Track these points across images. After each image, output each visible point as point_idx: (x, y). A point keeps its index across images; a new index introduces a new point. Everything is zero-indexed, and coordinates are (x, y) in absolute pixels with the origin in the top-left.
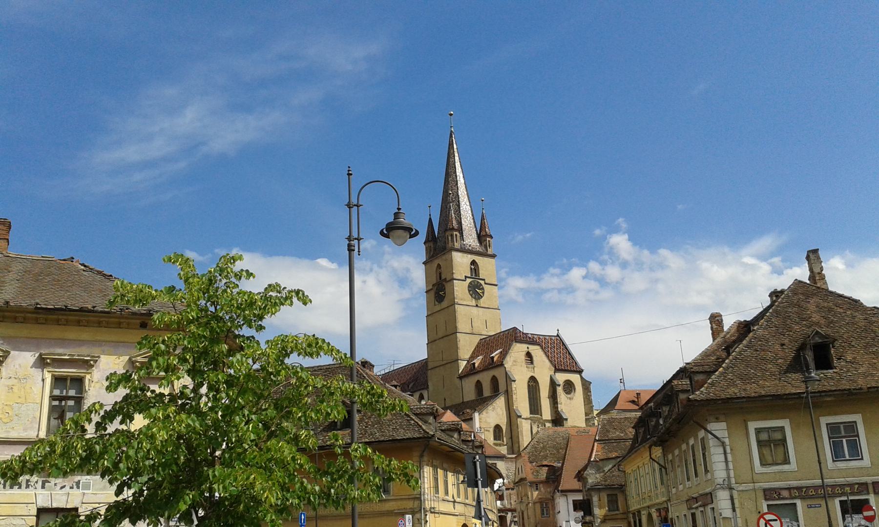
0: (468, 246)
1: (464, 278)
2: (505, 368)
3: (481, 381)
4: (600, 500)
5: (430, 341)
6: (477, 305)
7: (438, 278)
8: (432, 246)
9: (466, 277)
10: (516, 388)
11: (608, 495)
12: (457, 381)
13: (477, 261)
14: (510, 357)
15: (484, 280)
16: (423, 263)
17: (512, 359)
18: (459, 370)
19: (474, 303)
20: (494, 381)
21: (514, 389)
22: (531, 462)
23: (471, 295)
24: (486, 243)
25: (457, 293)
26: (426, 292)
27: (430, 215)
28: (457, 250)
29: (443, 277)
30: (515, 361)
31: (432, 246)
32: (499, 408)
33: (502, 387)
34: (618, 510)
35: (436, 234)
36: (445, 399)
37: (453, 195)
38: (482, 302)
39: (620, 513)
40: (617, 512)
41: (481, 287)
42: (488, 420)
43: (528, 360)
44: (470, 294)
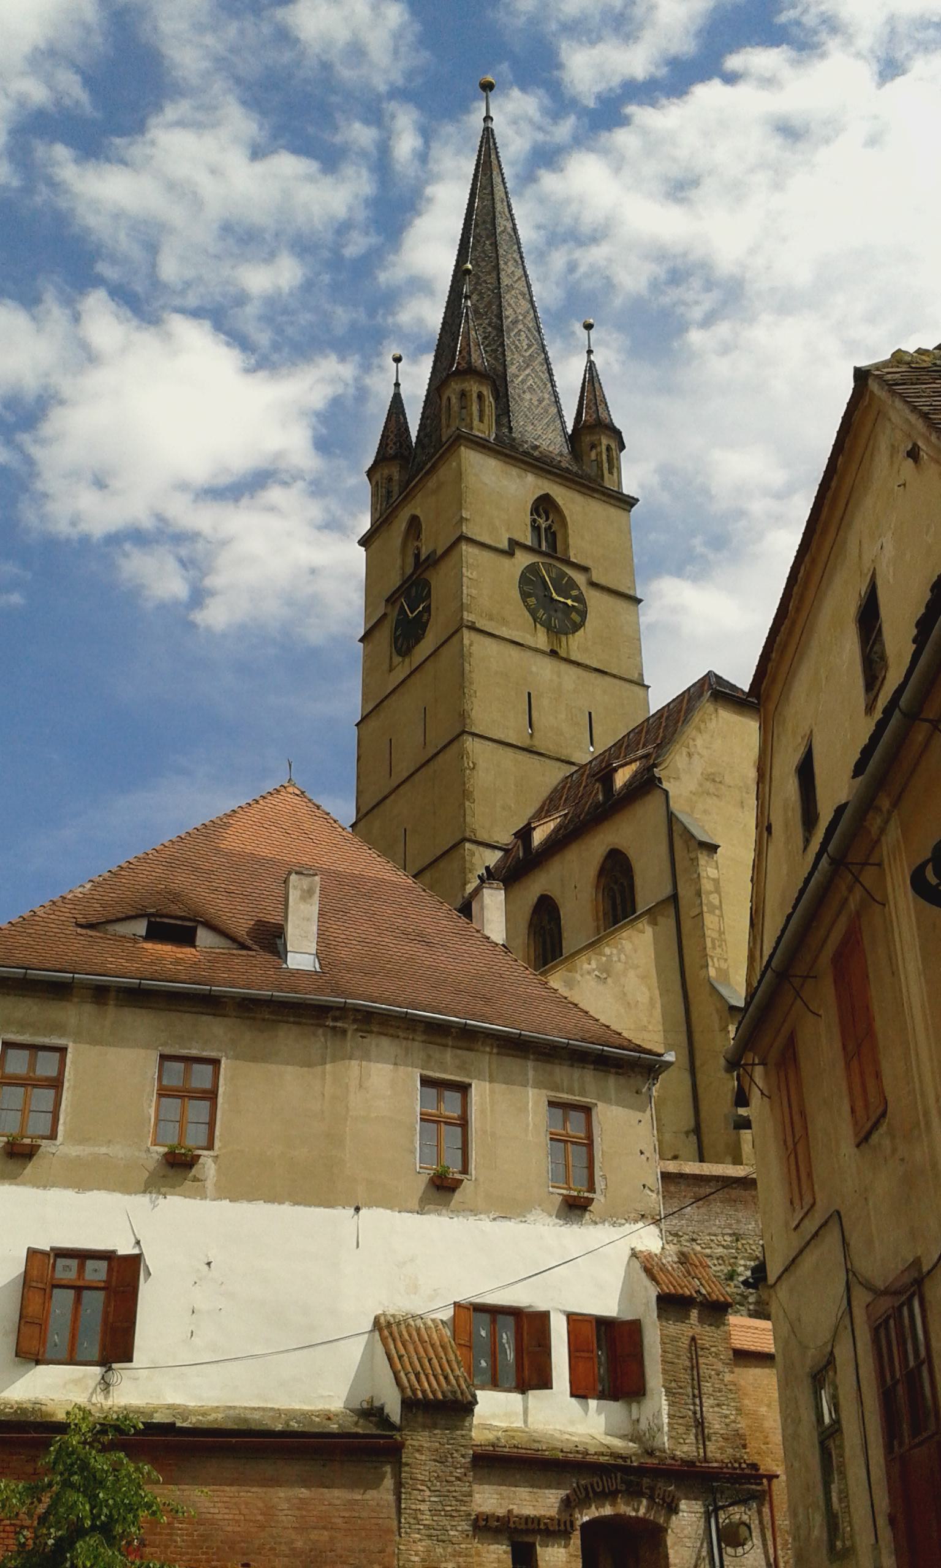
1: (504, 545)
2: (666, 792)
3: (556, 894)
5: (364, 811)
8: (396, 477)
9: (514, 544)
10: (716, 882)
13: (560, 501)
14: (690, 755)
15: (585, 569)
17: (699, 766)
18: (465, 884)
21: (707, 885)
23: (533, 613)
24: (600, 454)
25: (474, 592)
27: (397, 385)
28: (481, 445)
31: (396, 477)
32: (632, 974)
38: (576, 645)
41: (574, 593)
44: (528, 607)
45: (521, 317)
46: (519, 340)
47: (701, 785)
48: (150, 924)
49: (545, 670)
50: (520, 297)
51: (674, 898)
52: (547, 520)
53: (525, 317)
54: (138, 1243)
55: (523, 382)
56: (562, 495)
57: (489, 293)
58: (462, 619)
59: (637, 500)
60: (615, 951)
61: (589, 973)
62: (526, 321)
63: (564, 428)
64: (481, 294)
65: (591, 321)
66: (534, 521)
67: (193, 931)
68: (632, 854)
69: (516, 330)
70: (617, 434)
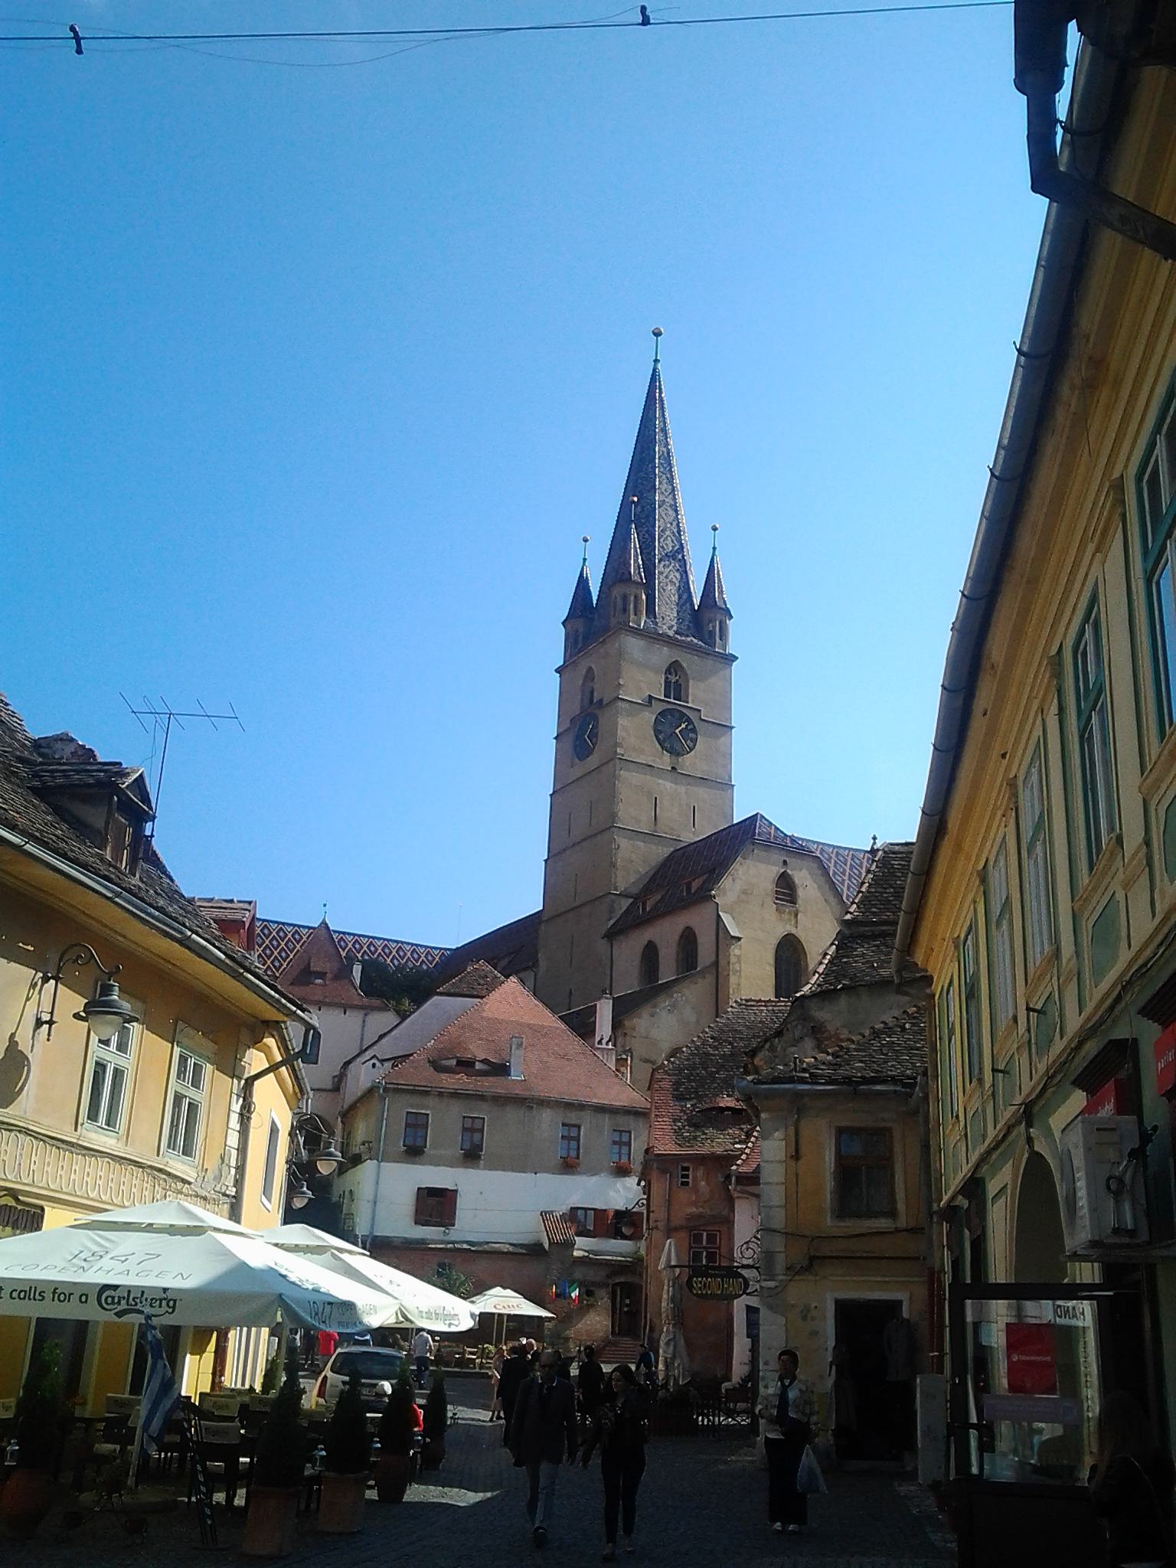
0: (665, 627)
3: (658, 942)
4: (796, 1156)
5: (553, 852)
7: (586, 701)
11: (842, 1133)
12: (602, 946)
13: (684, 665)
16: (556, 671)
17: (739, 886)
19: (665, 761)
20: (688, 939)
22: (680, 1098)
24: (714, 627)
25: (624, 734)
26: (556, 738)
28: (637, 632)
29: (596, 697)
30: (745, 892)
34: (893, 1214)
35: (595, 602)
36: (571, 992)
37: (642, 511)
39: (898, 1231)
40: (883, 1224)
42: (655, 1033)
44: (658, 740)
45: (669, 525)
46: (666, 544)
49: (667, 785)
50: (669, 509)
53: (671, 524)
55: (666, 577)
56: (686, 660)
58: (616, 751)
59: (737, 658)
61: (664, 1008)
62: (672, 528)
63: (692, 605)
64: (643, 507)
65: (718, 526)
66: (667, 678)
69: (665, 536)
70: (728, 611)
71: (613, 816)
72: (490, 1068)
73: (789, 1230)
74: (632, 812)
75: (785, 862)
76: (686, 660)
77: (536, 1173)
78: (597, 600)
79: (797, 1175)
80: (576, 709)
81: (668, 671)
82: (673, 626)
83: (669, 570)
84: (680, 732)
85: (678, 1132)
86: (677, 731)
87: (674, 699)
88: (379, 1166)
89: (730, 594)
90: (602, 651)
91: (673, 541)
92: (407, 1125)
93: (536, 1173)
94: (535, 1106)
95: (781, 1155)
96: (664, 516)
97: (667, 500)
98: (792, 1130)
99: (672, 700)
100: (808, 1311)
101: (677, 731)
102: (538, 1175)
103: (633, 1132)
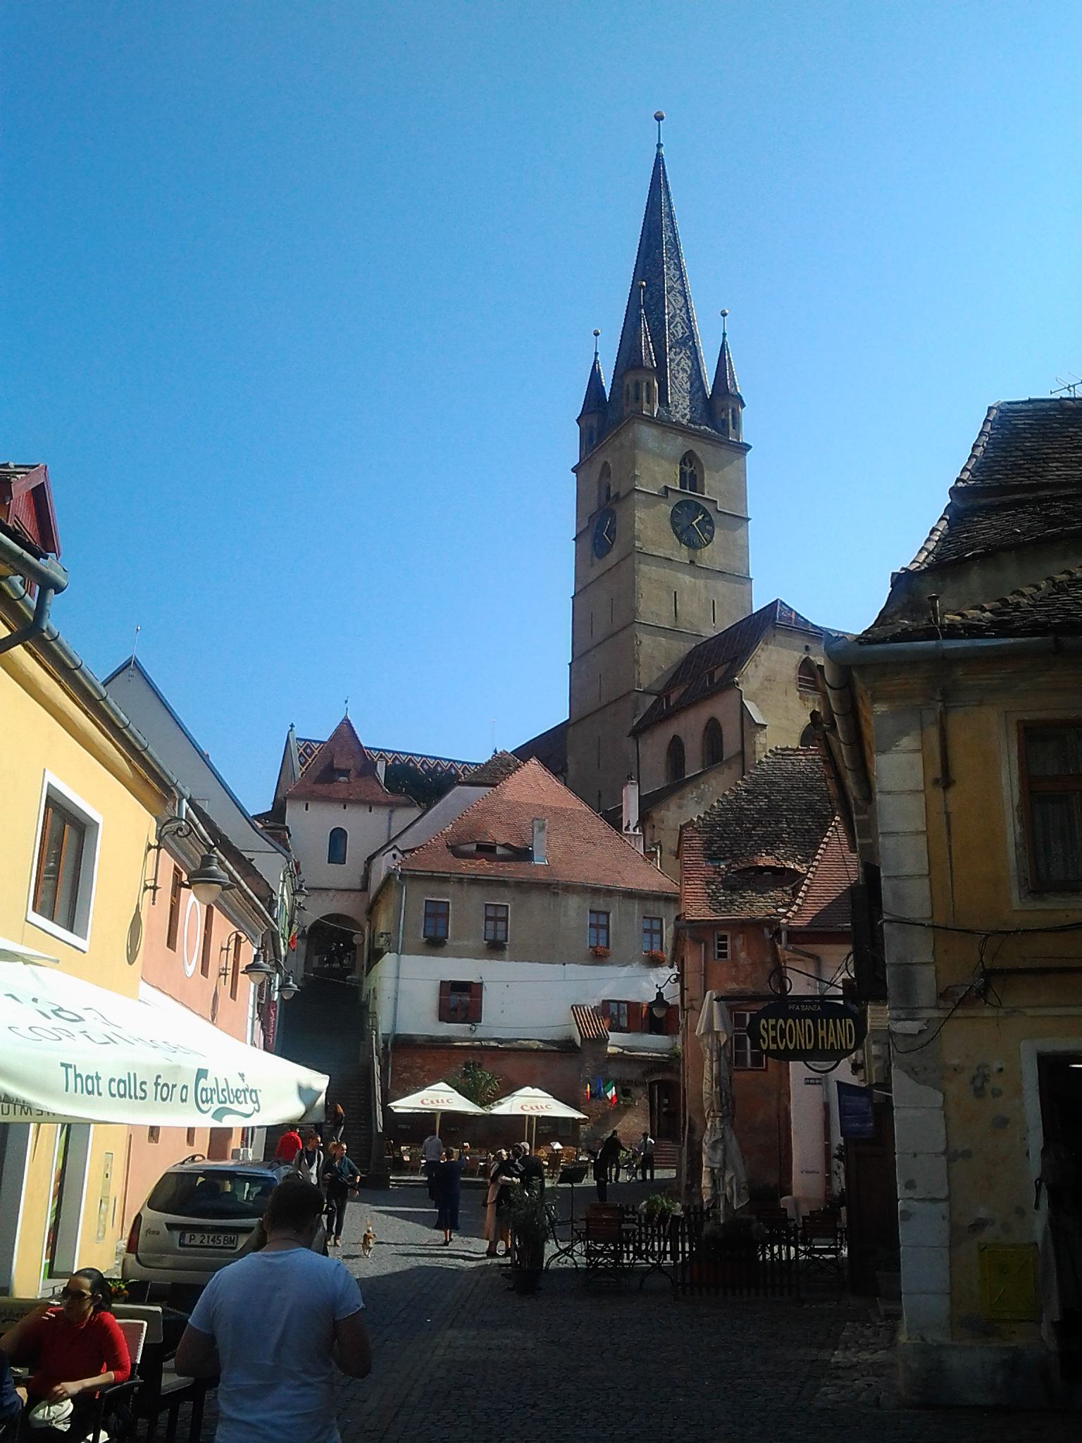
0: (678, 416)
4: (945, 780)
6: (692, 562)
7: (604, 497)
12: (628, 743)
13: (699, 454)
14: (756, 666)
16: (573, 470)
17: (762, 671)
20: (713, 731)
22: (712, 858)
26: (575, 539)
28: (650, 421)
33: (730, 745)
37: (651, 298)
38: (708, 555)
43: (807, 681)
44: (675, 533)
45: (678, 312)
46: (676, 331)
47: (762, 685)
48: (477, 845)
49: (687, 579)
50: (678, 295)
51: (742, 753)
52: (691, 467)
53: (681, 311)
54: (481, 978)
55: (678, 365)
56: (701, 449)
57: (657, 293)
58: (634, 545)
59: (750, 447)
60: (707, 786)
62: (682, 314)
64: (651, 294)
65: (727, 311)
67: (495, 847)
68: (722, 721)
69: (675, 323)
70: (739, 398)
71: (634, 611)
72: (511, 853)
73: (939, 920)
74: (653, 607)
75: (807, 648)
76: (701, 449)
77: (564, 964)
78: (610, 394)
79: (948, 814)
80: (593, 506)
81: (683, 462)
82: (686, 414)
83: (680, 357)
84: (696, 524)
85: (712, 897)
86: (694, 523)
87: (690, 490)
88: (399, 960)
89: (742, 383)
90: (617, 443)
91: (682, 328)
92: (427, 915)
93: (564, 964)
94: (560, 892)
95: (916, 778)
96: (673, 302)
97: (675, 286)
98: (933, 733)
99: (689, 492)
100: (986, 1078)
101: (694, 523)
102: (567, 965)
103: (664, 920)
